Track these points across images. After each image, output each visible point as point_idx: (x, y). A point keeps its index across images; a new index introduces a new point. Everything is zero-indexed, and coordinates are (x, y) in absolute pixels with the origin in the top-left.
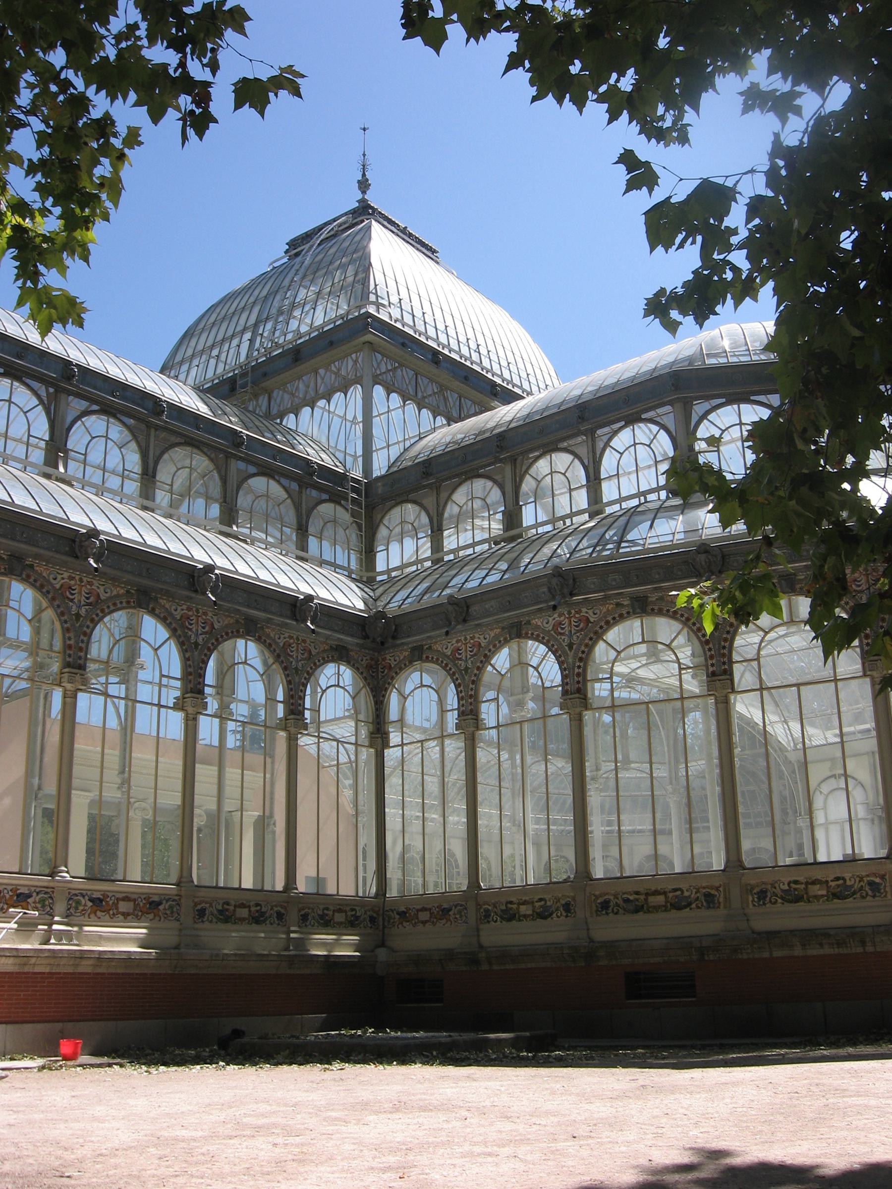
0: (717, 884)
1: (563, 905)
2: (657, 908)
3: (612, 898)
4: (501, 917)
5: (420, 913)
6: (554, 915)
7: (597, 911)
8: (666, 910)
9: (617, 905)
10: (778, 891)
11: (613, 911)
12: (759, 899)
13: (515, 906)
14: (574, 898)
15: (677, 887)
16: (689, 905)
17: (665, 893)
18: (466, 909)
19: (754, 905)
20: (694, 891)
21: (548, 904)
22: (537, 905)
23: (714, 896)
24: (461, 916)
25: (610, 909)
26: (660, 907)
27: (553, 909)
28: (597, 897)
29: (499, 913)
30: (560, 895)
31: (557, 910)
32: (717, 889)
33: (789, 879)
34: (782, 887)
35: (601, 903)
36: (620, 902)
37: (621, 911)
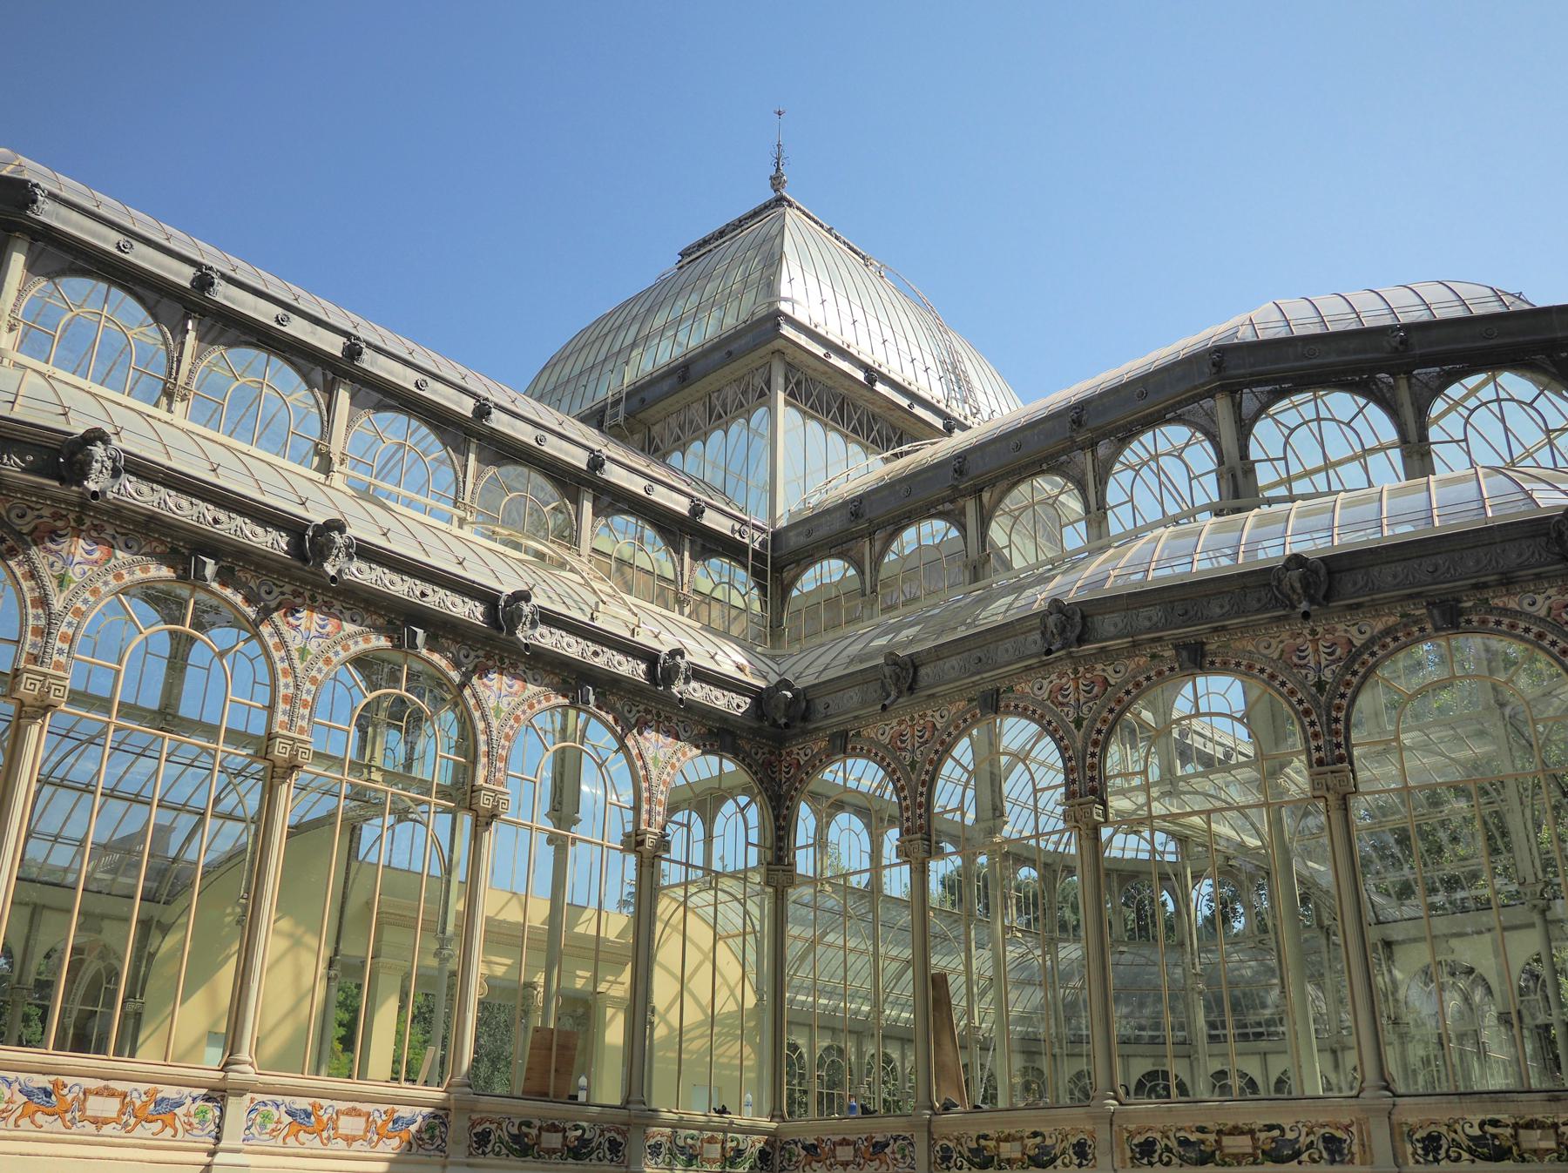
0: (1346, 1121)
1: (1074, 1146)
2: (1238, 1159)
3: (1158, 1136)
4: (970, 1161)
5: (839, 1148)
6: (1059, 1162)
7: (1132, 1159)
8: (1255, 1163)
9: (1168, 1149)
10: (1461, 1138)
11: (1161, 1160)
12: (1426, 1151)
13: (992, 1144)
14: (1092, 1135)
15: (1274, 1122)
16: (1296, 1155)
17: (1251, 1132)
18: (911, 1144)
19: (1417, 1162)
20: (1304, 1130)
21: (1048, 1142)
22: (1030, 1142)
23: (1341, 1141)
24: (904, 1157)
25: (1156, 1156)
26: (1244, 1155)
27: (1058, 1151)
28: (1131, 1135)
29: (966, 1153)
30: (1068, 1128)
31: (1063, 1153)
32: (1347, 1129)
33: (1481, 1117)
34: (1468, 1131)
35: (1140, 1145)
36: (1173, 1144)
37: (1175, 1160)
